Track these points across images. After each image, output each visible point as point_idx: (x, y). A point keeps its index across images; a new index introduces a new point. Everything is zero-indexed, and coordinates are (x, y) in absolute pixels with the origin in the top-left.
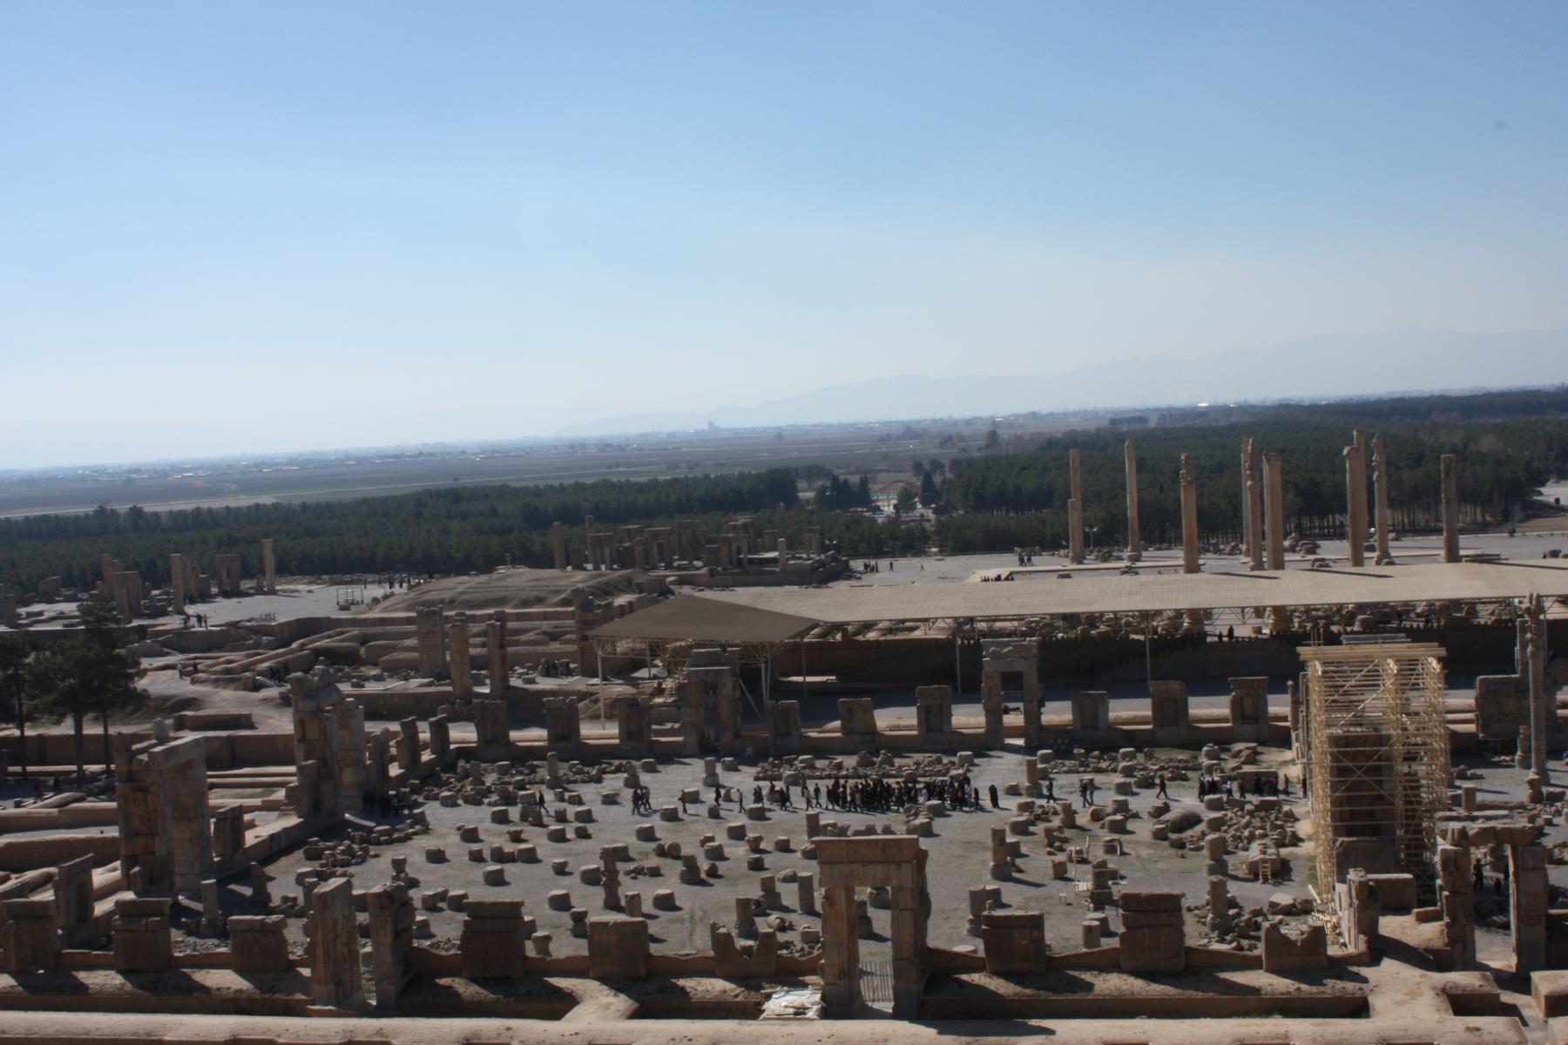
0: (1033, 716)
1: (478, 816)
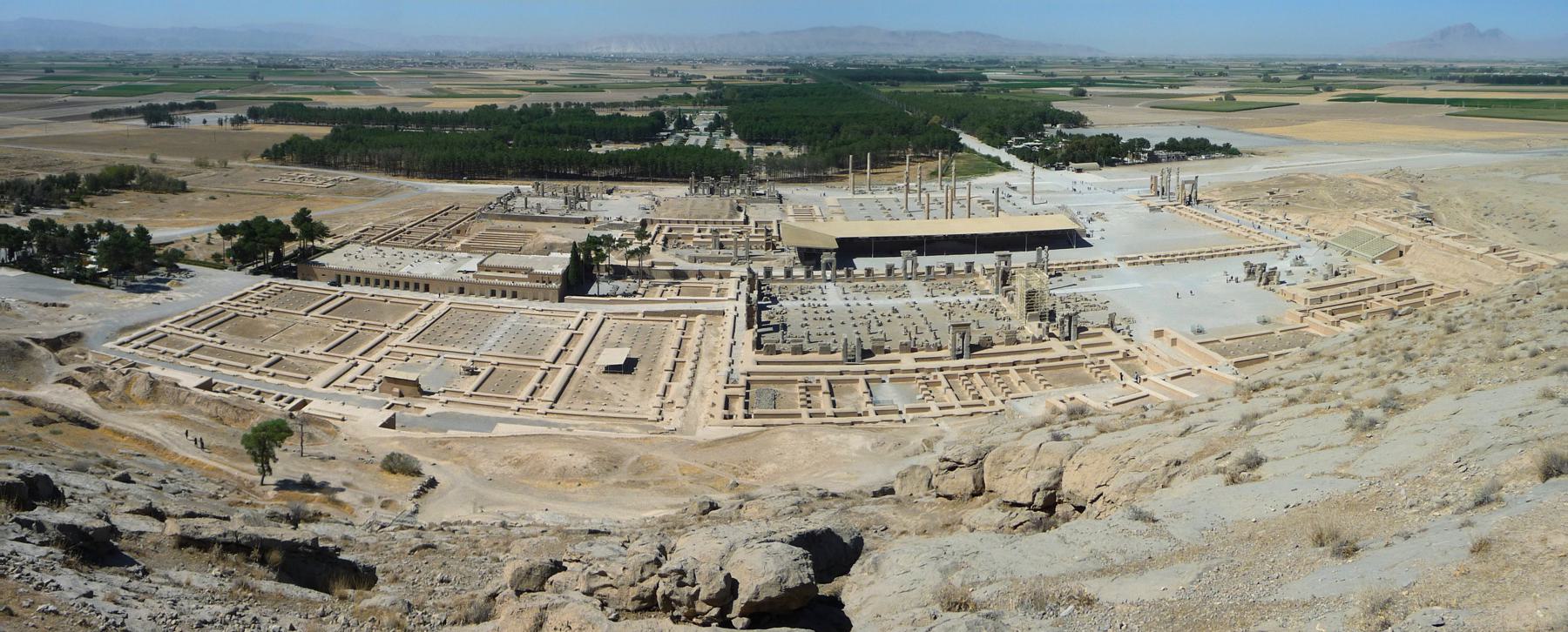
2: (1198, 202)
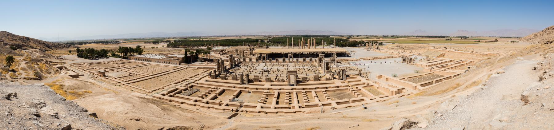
0: (293, 61)
1: (246, 67)
2: (380, 49)
